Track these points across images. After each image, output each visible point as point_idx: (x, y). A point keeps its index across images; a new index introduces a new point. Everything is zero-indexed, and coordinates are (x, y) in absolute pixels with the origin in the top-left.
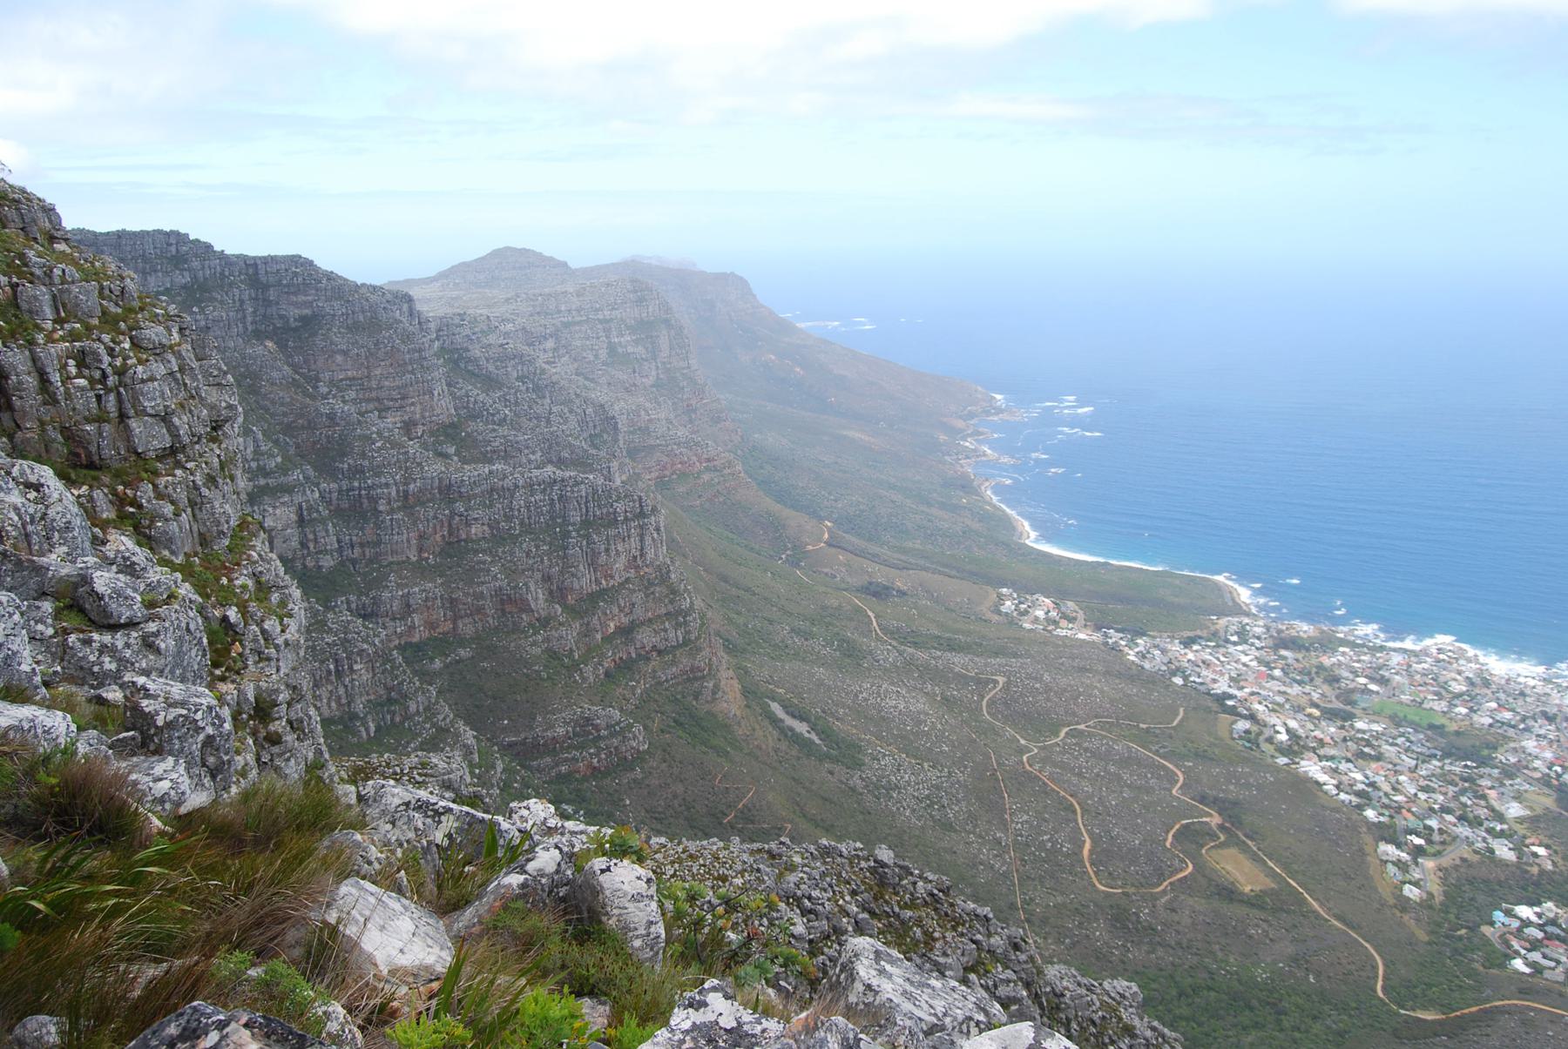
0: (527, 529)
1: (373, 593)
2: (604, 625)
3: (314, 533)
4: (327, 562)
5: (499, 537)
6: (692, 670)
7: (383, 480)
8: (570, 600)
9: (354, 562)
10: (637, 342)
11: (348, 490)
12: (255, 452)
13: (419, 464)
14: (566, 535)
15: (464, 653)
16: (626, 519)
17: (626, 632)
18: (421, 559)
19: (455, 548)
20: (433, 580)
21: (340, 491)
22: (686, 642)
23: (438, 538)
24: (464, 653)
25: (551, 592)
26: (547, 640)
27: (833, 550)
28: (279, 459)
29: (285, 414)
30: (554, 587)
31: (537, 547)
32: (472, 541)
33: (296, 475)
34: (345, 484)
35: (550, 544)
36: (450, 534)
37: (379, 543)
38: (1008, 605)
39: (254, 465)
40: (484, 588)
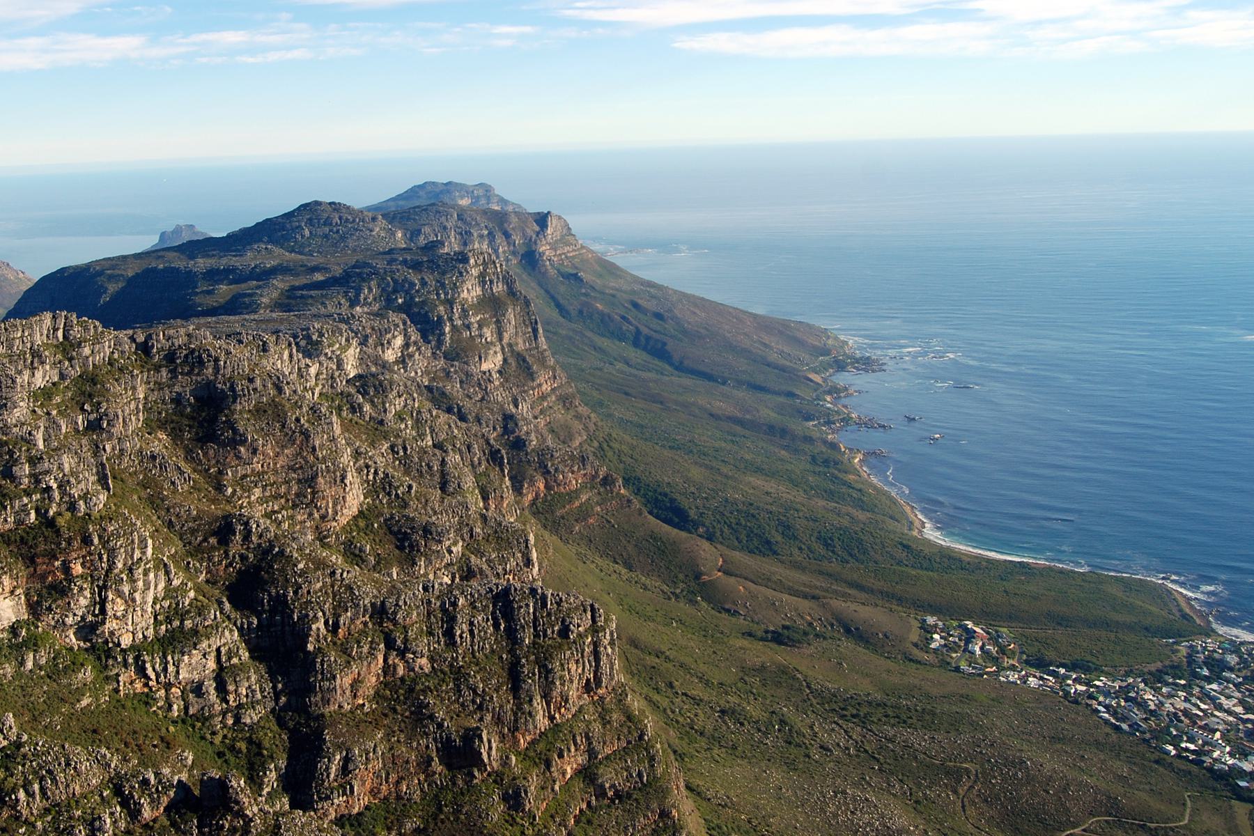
16: (580, 635)
28: (192, 594)
39: (166, 604)
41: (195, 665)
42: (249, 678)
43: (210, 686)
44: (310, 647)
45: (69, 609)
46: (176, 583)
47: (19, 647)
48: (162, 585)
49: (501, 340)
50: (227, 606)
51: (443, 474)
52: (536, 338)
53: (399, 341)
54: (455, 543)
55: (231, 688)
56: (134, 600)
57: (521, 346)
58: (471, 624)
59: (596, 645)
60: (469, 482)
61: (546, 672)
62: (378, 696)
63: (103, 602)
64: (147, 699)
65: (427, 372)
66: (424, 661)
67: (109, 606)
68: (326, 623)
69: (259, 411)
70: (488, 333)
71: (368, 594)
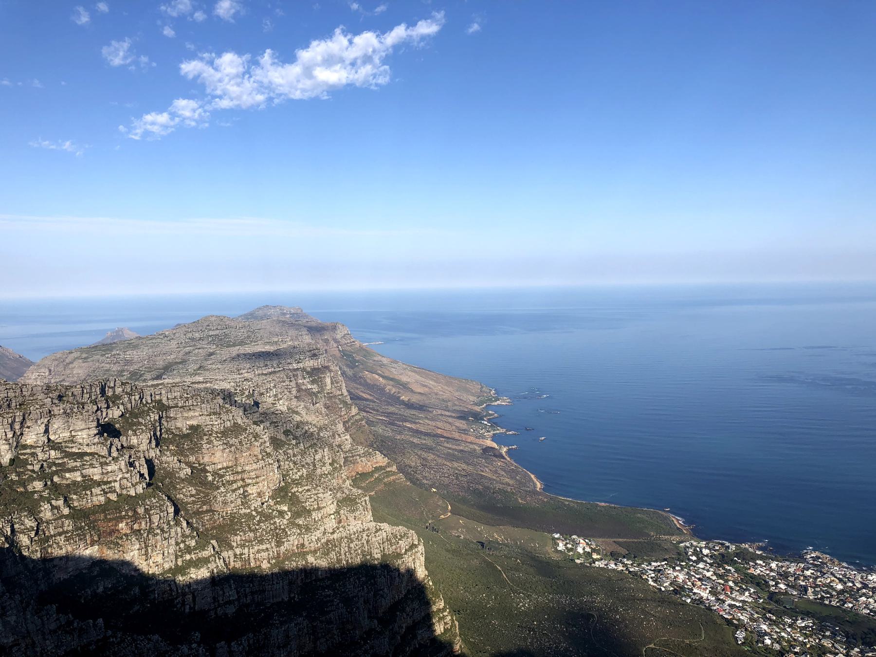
2: (400, 627)
3: (222, 589)
4: (231, 610)
7: (264, 547)
10: (313, 382)
11: (241, 554)
12: (183, 536)
13: (284, 530)
18: (291, 598)
20: (301, 616)
21: (235, 555)
25: (369, 611)
26: (372, 647)
29: (194, 502)
30: (371, 607)
31: (359, 579)
32: (320, 580)
34: (238, 551)
38: (561, 547)
39: (182, 546)
58: (349, 547)
60: (327, 468)
63: (146, 547)
65: (288, 409)
69: (225, 433)
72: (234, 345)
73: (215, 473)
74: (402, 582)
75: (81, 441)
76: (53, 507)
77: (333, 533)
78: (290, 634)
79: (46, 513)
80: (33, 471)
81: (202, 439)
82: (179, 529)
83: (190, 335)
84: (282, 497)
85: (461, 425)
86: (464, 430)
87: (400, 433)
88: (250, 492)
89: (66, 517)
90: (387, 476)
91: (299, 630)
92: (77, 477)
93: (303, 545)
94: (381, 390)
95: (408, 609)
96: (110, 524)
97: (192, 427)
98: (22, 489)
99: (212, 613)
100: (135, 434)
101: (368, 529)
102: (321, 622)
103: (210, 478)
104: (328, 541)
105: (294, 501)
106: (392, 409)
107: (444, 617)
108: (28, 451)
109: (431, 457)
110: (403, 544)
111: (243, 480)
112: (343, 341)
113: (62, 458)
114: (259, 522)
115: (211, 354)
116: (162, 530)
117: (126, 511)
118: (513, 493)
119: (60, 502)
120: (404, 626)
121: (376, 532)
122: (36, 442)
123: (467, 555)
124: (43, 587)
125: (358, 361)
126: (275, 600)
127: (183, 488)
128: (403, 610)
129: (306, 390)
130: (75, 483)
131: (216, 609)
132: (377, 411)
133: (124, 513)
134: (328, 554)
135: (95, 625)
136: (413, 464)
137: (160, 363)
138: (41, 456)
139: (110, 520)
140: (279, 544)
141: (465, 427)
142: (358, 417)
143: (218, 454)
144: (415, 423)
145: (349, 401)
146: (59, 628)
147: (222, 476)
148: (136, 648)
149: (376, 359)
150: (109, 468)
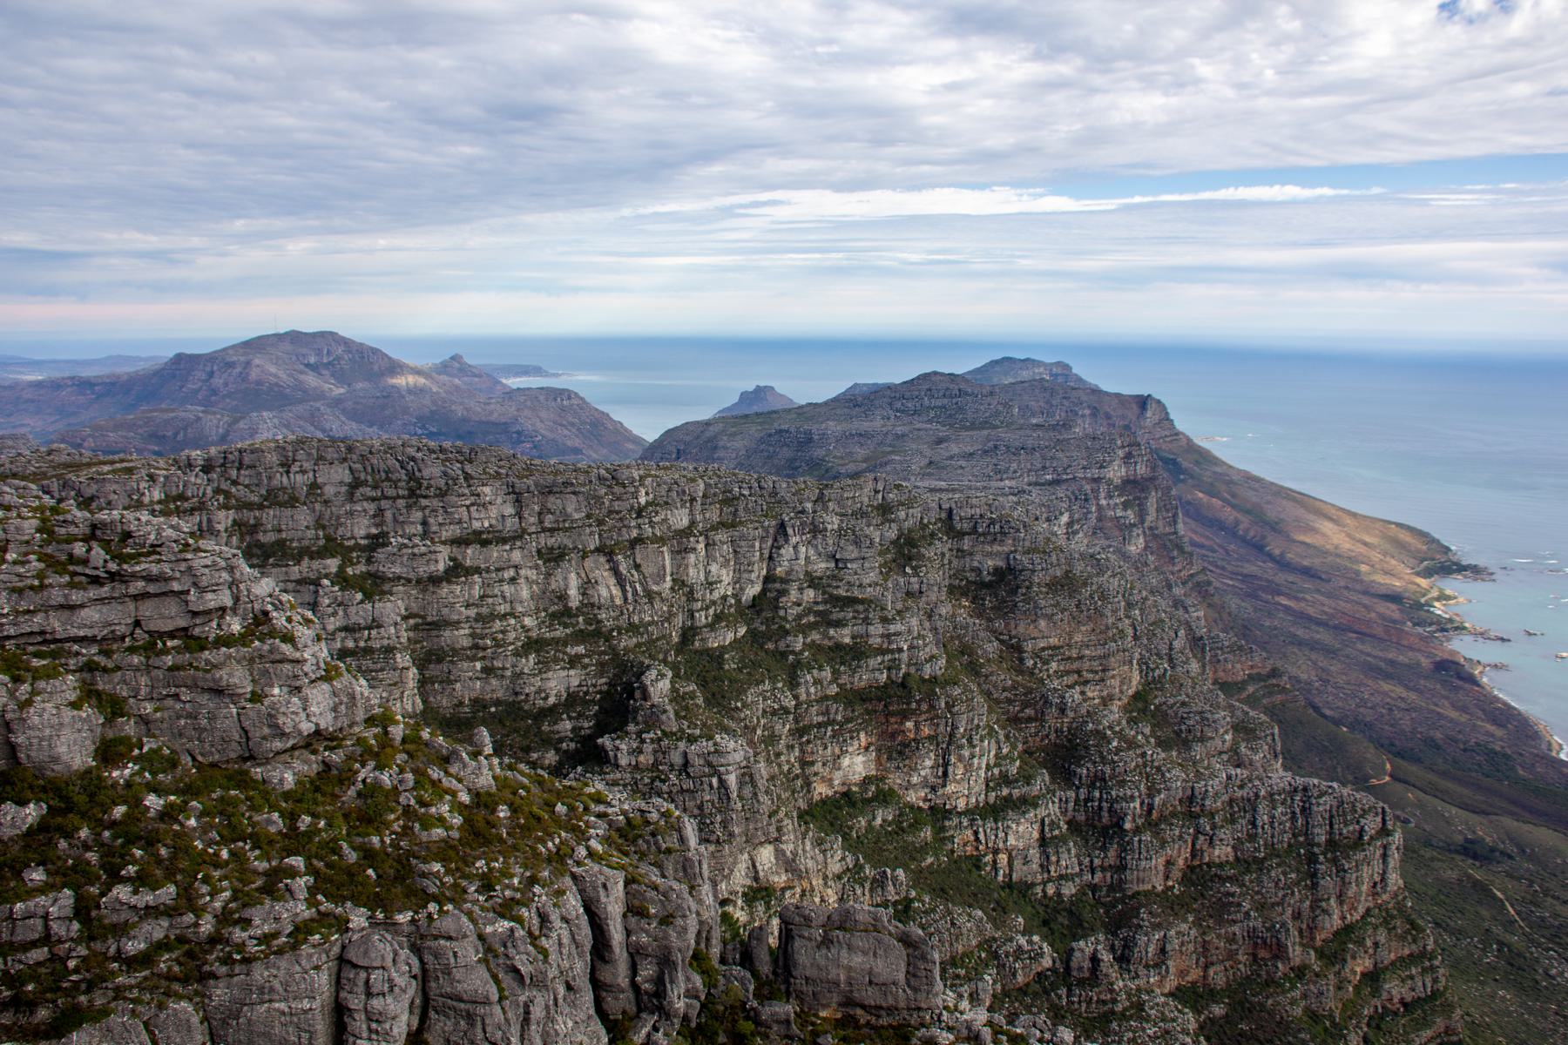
0: (1273, 851)
1: (1123, 933)
2: (1355, 973)
4: (1069, 890)
5: (1246, 864)
6: (1446, 1033)
7: (1129, 793)
8: (1318, 943)
9: (1094, 888)
10: (1126, 506)
11: (1087, 800)
12: (996, 756)
13: (1158, 769)
14: (1312, 859)
15: (1218, 1010)
16: (1372, 838)
17: (1373, 978)
19: (1199, 876)
20: (1185, 920)
22: (1435, 994)
23: (1181, 862)
24: (1218, 1010)
25: (1301, 931)
26: (1305, 996)
27: (1399, 787)
29: (1009, 701)
31: (1285, 874)
33: (1037, 787)
35: (1298, 871)
36: (1193, 855)
37: (1121, 867)
39: (996, 771)
40: (1236, 929)
41: (1022, 832)
42: (1069, 851)
43: (1034, 853)
44: (1128, 826)
45: (915, 769)
46: (1005, 751)
47: (870, 801)
48: (993, 753)
49: (1142, 521)
50: (1047, 778)
51: (1171, 660)
52: (1175, 522)
53: (1065, 519)
54: (1226, 732)
55: (1054, 859)
56: (971, 765)
57: (1163, 528)
59: (1385, 847)
61: (1341, 870)
62: (1185, 880)
63: (946, 765)
64: (976, 862)
66: (1229, 849)
67: (950, 769)
68: (1142, 804)
69: (1054, 586)
70: (1131, 516)
71: (1177, 778)
72: (973, 427)
73: (1036, 655)
74: (1360, 893)
75: (851, 579)
76: (815, 683)
77: (1241, 787)
78: (1168, 947)
79: (808, 687)
80: (785, 619)
81: (1014, 591)
82: (994, 746)
83: (898, 405)
84: (1139, 711)
85: (1388, 613)
86: (1394, 622)
87: (1270, 615)
88: (1090, 694)
89: (836, 698)
90: (1271, 694)
91: (1182, 944)
92: (845, 636)
93: (1191, 798)
94: (1230, 531)
95: (1369, 943)
96: (893, 720)
97: (997, 571)
98: (770, 646)
99: (1039, 890)
100: (916, 574)
101: (1305, 789)
102: (1219, 936)
103: (1030, 663)
104: (1231, 801)
105: (1160, 718)
106: (1250, 569)
107: (1432, 969)
108: (777, 585)
109: (1335, 667)
110: (1371, 825)
111: (1079, 672)
112: (1159, 433)
113: (825, 602)
114: (1118, 750)
115: (940, 441)
116: (970, 740)
117: (918, 702)
118: (1505, 755)
119: (827, 674)
120: (1358, 969)
121: (1320, 796)
122: (788, 573)
123: (1432, 859)
124: (803, 805)
125: (1184, 472)
126: (1142, 888)
127: (992, 674)
128: (1360, 942)
129: (1111, 519)
130: (839, 647)
131: (1044, 883)
132: (1223, 568)
133: (914, 705)
134: (1233, 821)
135: (895, 879)
136: (1304, 677)
137: (861, 452)
138: (794, 594)
139: (892, 714)
140: (1152, 791)
141: (1397, 615)
142: (1201, 578)
143: (1042, 623)
144: (1297, 599)
145: (1188, 549)
146: (844, 872)
147: (1046, 662)
148: (953, 924)
149: (1218, 470)
150: (893, 628)
